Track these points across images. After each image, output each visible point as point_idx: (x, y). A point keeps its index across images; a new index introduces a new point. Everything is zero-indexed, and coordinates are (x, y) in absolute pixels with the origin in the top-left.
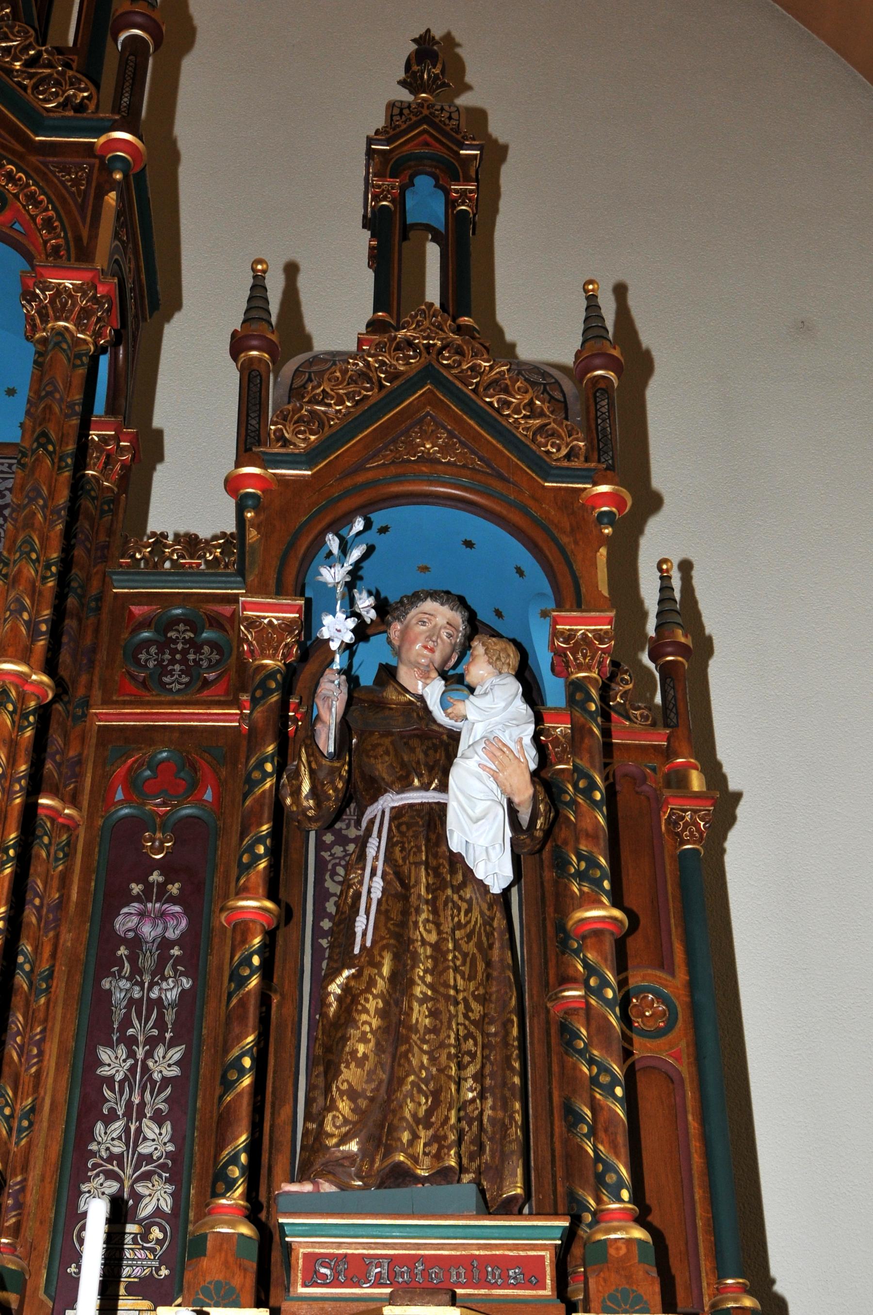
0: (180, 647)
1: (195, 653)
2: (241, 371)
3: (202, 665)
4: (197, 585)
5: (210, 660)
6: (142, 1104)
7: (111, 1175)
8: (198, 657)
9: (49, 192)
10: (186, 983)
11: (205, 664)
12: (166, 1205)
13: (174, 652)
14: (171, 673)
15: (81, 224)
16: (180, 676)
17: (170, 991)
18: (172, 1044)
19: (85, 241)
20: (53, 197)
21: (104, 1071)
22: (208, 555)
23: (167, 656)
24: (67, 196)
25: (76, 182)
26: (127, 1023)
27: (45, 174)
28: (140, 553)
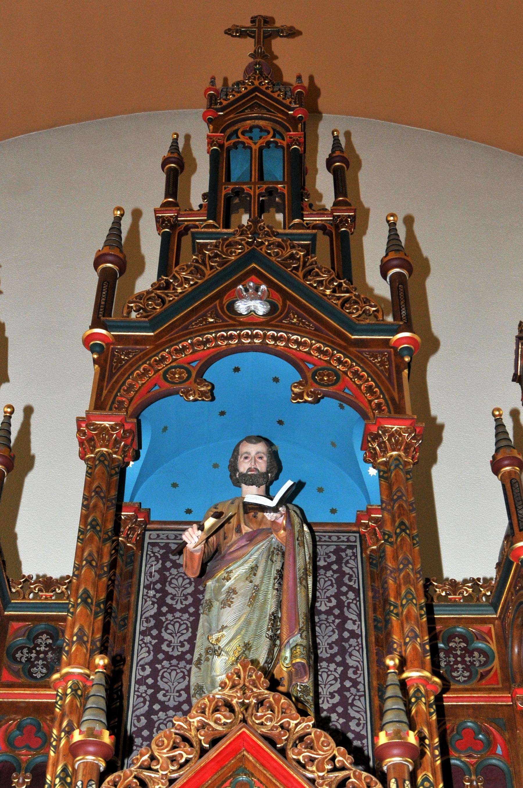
0: (459, 653)
1: (469, 657)
2: (501, 480)
3: (475, 665)
4: (456, 612)
5: (480, 661)
8: (472, 659)
9: (368, 370)
11: (477, 664)
13: (456, 656)
14: (457, 670)
15: (391, 389)
16: (463, 672)
19: (397, 399)
20: (371, 373)
22: (57, 590)
23: (452, 659)
24: (379, 372)
25: (382, 363)
27: (363, 359)
28: (59, 589)
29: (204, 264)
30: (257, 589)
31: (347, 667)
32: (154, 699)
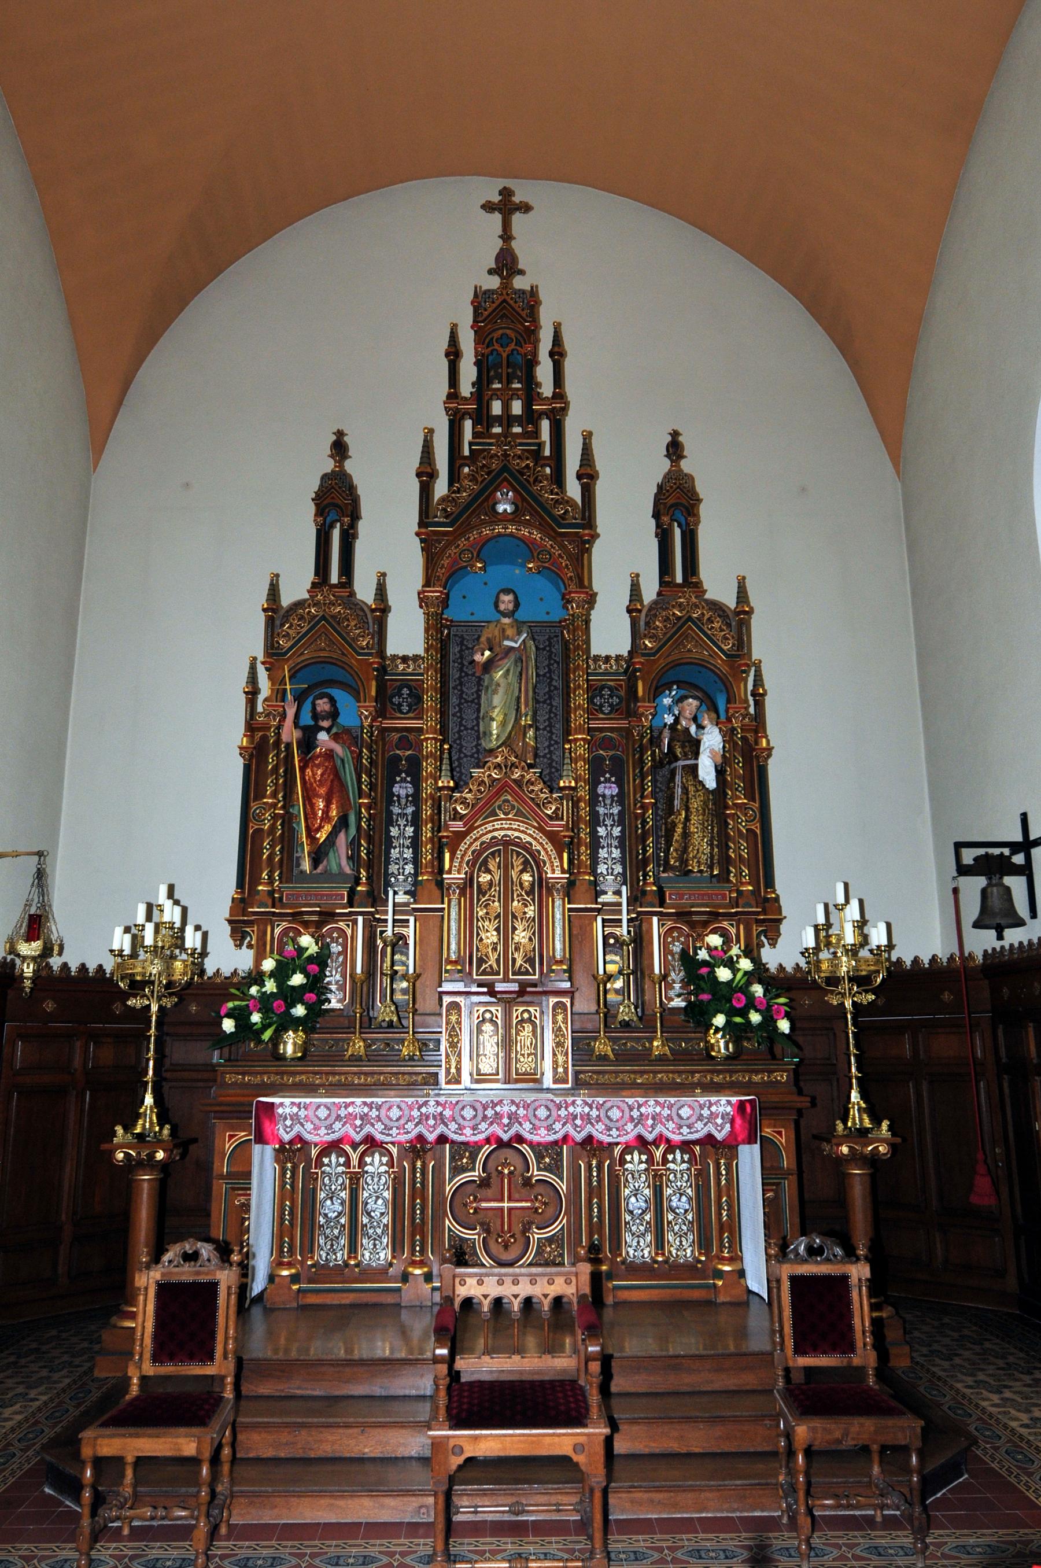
29: (477, 472)
30: (509, 684)
31: (552, 706)
32: (461, 725)
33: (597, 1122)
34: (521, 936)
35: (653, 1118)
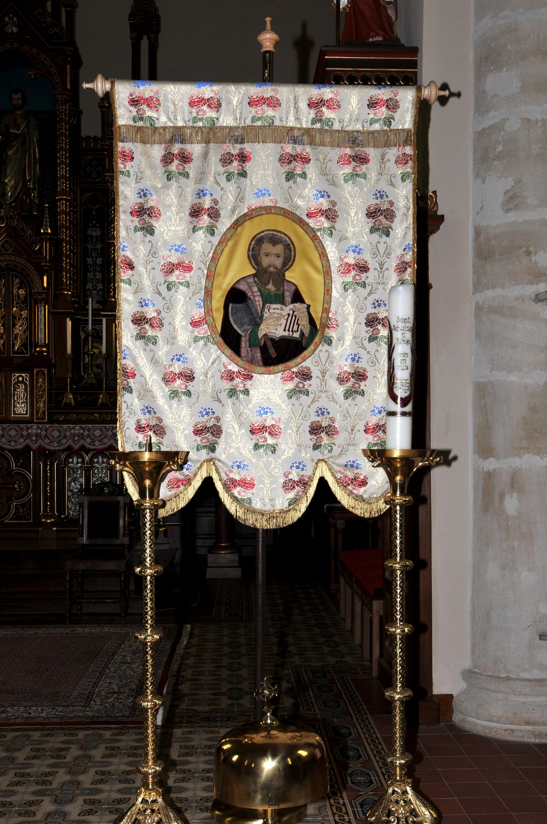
6: (96, 269)
7: (91, 282)
10: (102, 245)
12: (102, 287)
17: (99, 246)
18: (100, 257)
21: (89, 263)
26: (91, 253)
33: (45, 438)
34: (19, 329)
35: (36, 436)
